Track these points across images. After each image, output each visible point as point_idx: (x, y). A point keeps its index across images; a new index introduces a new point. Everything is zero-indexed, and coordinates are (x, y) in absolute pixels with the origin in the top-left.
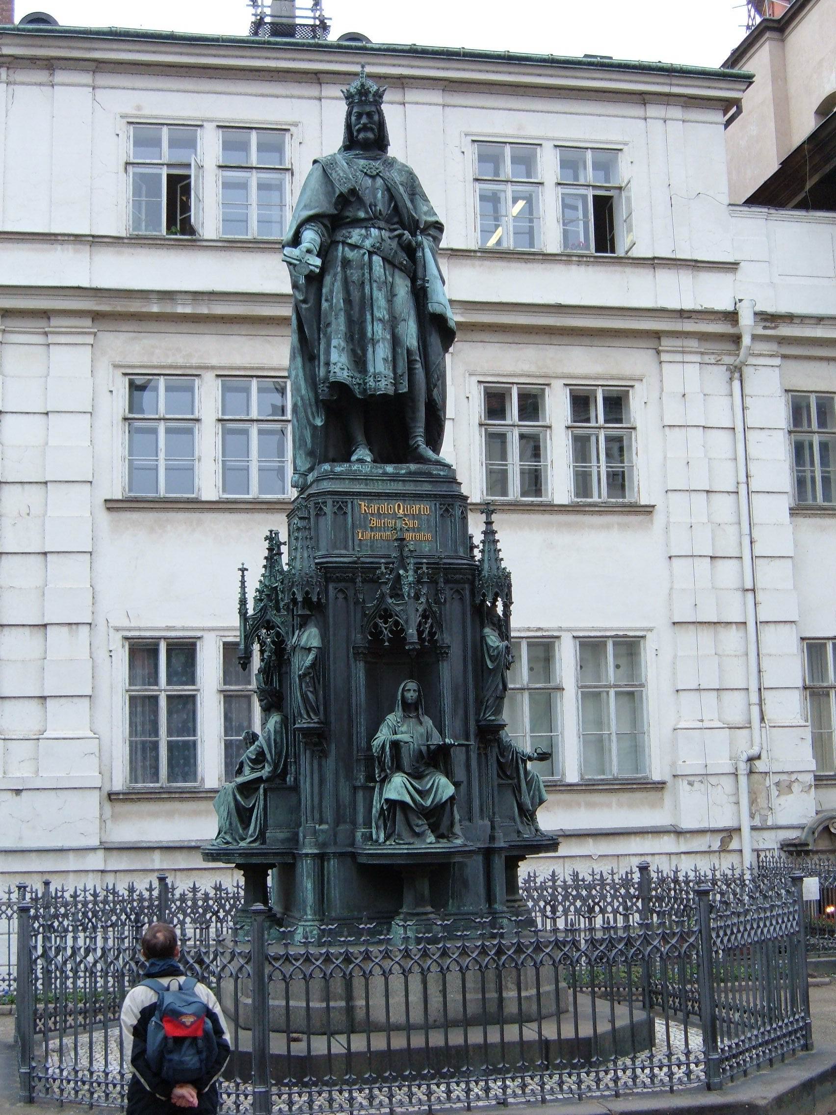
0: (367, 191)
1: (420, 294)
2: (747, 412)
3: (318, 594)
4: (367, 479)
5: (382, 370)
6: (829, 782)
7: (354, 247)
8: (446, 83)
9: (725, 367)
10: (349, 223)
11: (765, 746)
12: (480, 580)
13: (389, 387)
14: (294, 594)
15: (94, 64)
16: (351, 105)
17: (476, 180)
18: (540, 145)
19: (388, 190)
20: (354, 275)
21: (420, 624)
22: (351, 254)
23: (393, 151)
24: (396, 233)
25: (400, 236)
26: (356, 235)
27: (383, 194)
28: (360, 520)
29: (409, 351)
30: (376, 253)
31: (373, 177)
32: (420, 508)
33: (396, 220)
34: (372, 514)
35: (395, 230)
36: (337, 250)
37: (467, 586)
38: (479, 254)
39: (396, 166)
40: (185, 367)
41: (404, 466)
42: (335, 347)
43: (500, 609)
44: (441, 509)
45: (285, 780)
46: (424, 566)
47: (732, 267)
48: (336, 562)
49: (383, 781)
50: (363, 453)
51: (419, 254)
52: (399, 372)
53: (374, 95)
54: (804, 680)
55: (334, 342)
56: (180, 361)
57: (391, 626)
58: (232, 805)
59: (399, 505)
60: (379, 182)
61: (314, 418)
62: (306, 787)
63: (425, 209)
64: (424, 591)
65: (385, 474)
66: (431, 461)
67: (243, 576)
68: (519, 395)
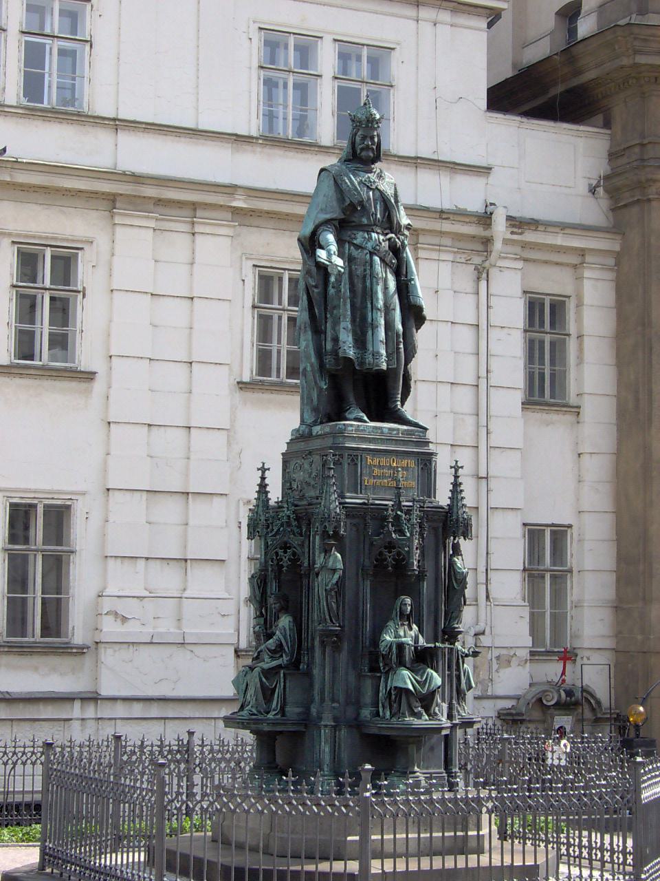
2: (491, 311)
6: (541, 658)
7: (358, 247)
9: (473, 267)
10: (353, 226)
11: (489, 623)
18: (321, 38)
33: (387, 226)
34: (375, 466)
35: (387, 234)
38: (260, 141)
45: (299, 669)
47: (485, 171)
49: (387, 673)
54: (524, 563)
57: (394, 555)
58: (259, 685)
59: (393, 460)
62: (316, 671)
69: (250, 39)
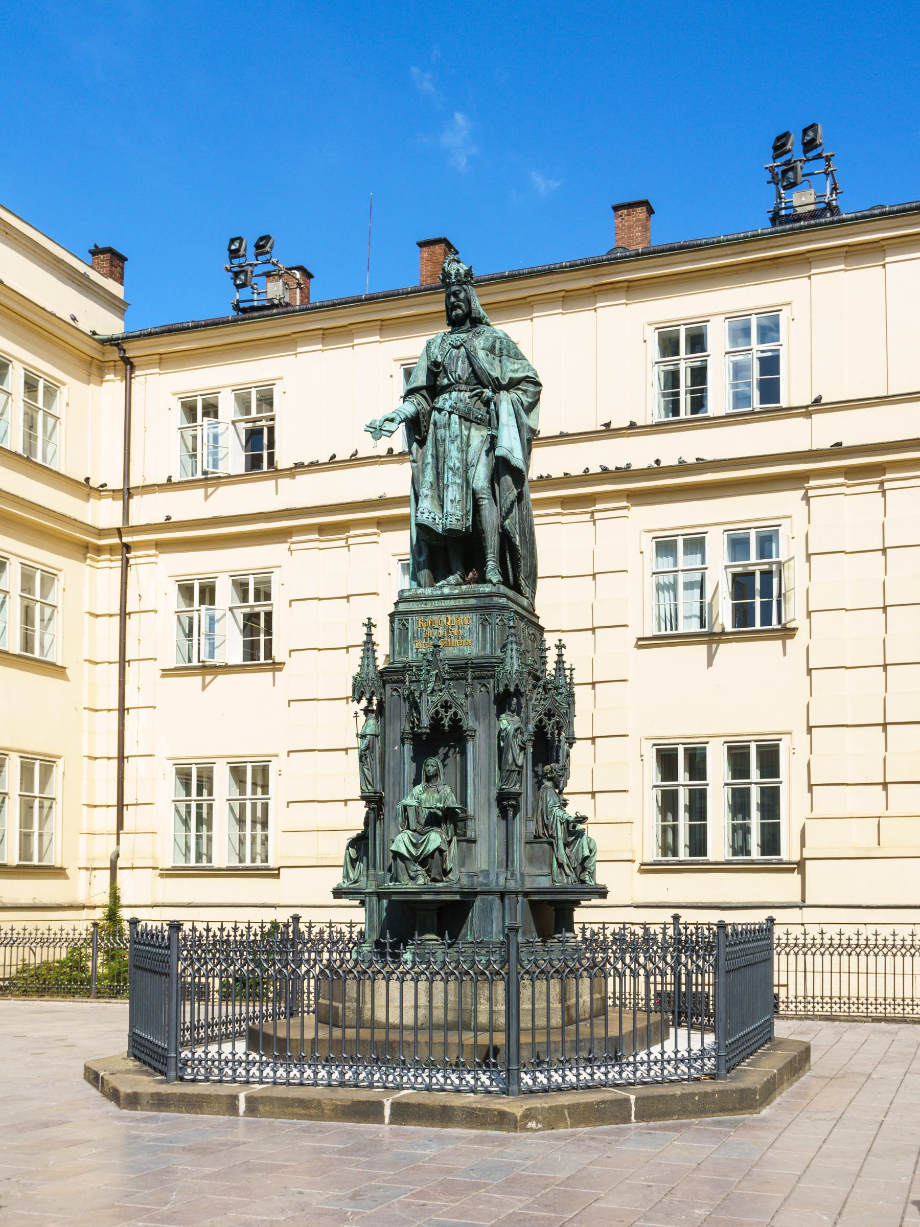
5: (449, 509)
7: (440, 410)
21: (437, 713)
25: (479, 395)
27: (463, 363)
29: (474, 493)
31: (458, 348)
39: (487, 334)
51: (492, 407)
60: (463, 349)
65: (442, 595)
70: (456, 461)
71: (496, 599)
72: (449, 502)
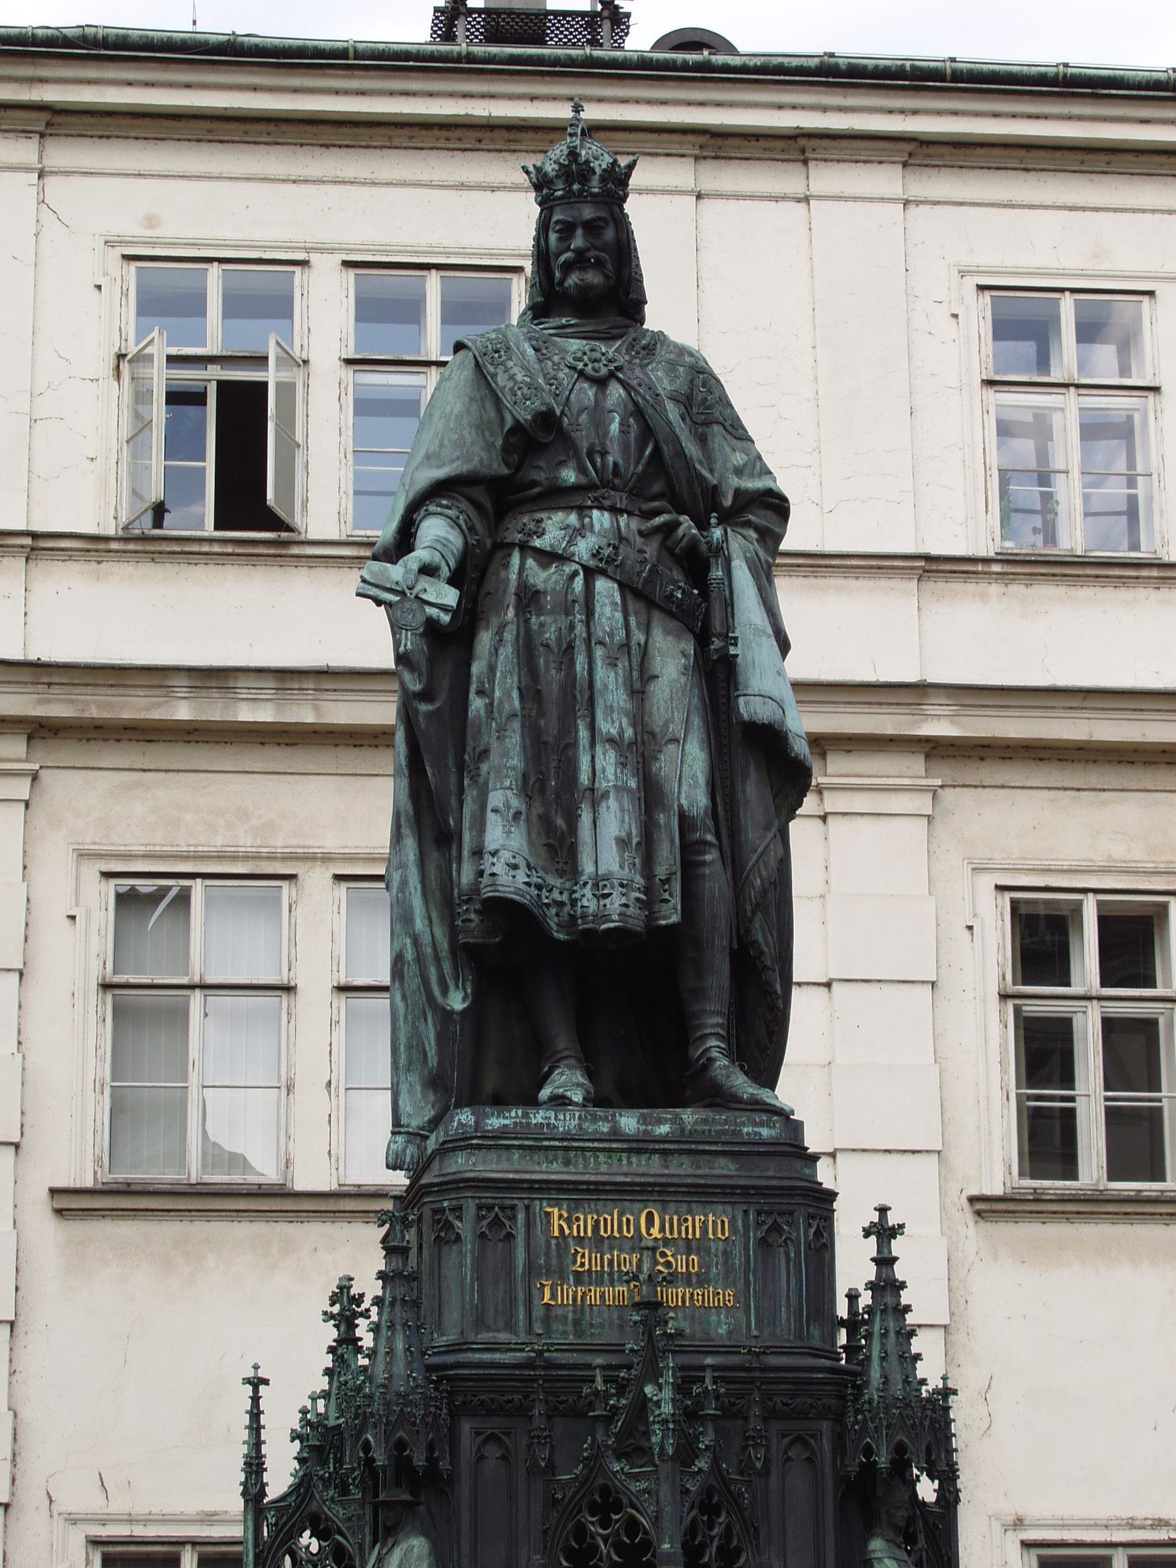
0: (584, 417)
1: (717, 675)
3: (431, 1447)
4: (569, 1146)
5: (615, 868)
7: (548, 557)
8: (910, 147)
12: (857, 1412)
13: (631, 911)
14: (367, 1447)
15: (45, 116)
16: (546, 204)
17: (990, 383)
18: (1151, 293)
19: (638, 412)
20: (550, 628)
21: (693, 1527)
22: (541, 577)
23: (654, 319)
24: (658, 520)
25: (670, 528)
26: (554, 529)
28: (547, 1255)
30: (603, 573)
31: (601, 383)
32: (704, 1224)
33: (657, 488)
34: (580, 1240)
35: (656, 513)
36: (506, 566)
37: (825, 1426)
38: (996, 568)
39: (662, 353)
40: (257, 857)
41: (667, 1114)
42: (495, 811)
43: (927, 1490)
44: (759, 1225)
46: (708, 1376)
48: (480, 1365)
50: (567, 1080)
51: (717, 573)
52: (661, 871)
53: (603, 179)
55: (496, 799)
56: (246, 842)
57: (617, 1532)
59: (650, 1216)
60: (616, 392)
61: (445, 992)
63: (739, 459)
64: (705, 1442)
65: (616, 1134)
66: (740, 1100)
67: (256, 1399)
68: (1101, 919)
69: (955, 316)
70: (625, 721)
71: (798, 1164)
72: (614, 847)
